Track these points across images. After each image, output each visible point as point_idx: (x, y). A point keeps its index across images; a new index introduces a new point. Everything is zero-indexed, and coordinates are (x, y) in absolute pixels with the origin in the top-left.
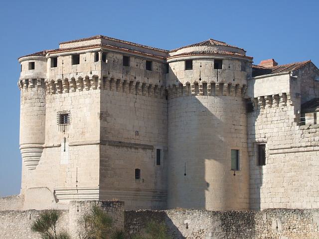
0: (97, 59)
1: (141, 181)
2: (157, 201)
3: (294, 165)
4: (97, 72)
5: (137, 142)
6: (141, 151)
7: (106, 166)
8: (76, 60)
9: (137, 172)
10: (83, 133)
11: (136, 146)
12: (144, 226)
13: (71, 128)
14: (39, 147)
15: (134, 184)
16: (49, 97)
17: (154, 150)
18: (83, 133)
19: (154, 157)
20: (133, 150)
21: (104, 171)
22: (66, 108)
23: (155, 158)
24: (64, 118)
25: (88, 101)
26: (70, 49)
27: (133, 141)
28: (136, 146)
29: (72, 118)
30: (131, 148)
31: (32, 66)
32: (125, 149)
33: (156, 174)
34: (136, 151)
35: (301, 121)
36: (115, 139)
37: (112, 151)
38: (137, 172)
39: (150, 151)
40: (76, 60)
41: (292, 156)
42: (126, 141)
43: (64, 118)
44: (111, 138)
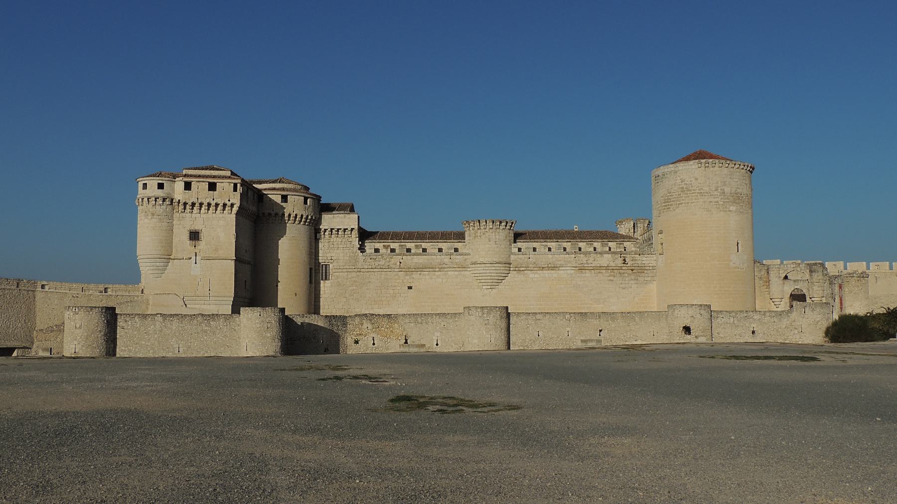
0: (235, 190)
3: (355, 281)
4: (236, 199)
8: (212, 187)
10: (216, 250)
13: (202, 245)
14: (167, 257)
16: (176, 215)
18: (216, 250)
22: (197, 227)
24: (195, 236)
25: (221, 223)
26: (207, 177)
29: (201, 235)
31: (161, 186)
35: (362, 249)
40: (212, 187)
41: (354, 274)
43: (195, 236)
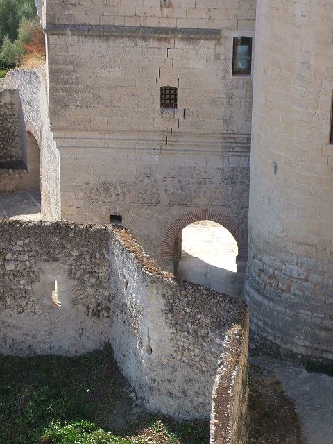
1: (179, 115)
2: (239, 156)
5: (165, 24)
6: (178, 45)
7: (67, 83)
9: (168, 98)
11: (163, 34)
12: (45, 257)
15: (158, 120)
17: (222, 40)
19: (222, 57)
20: (152, 43)
21: (61, 93)
23: (226, 59)
27: (152, 23)
28: (163, 34)
30: (144, 39)
32: (127, 42)
33: (230, 96)
34: (163, 44)
36: (92, 21)
37: (87, 48)
38: (168, 98)
39: (211, 44)
42: (130, 23)
44: (80, 17)
